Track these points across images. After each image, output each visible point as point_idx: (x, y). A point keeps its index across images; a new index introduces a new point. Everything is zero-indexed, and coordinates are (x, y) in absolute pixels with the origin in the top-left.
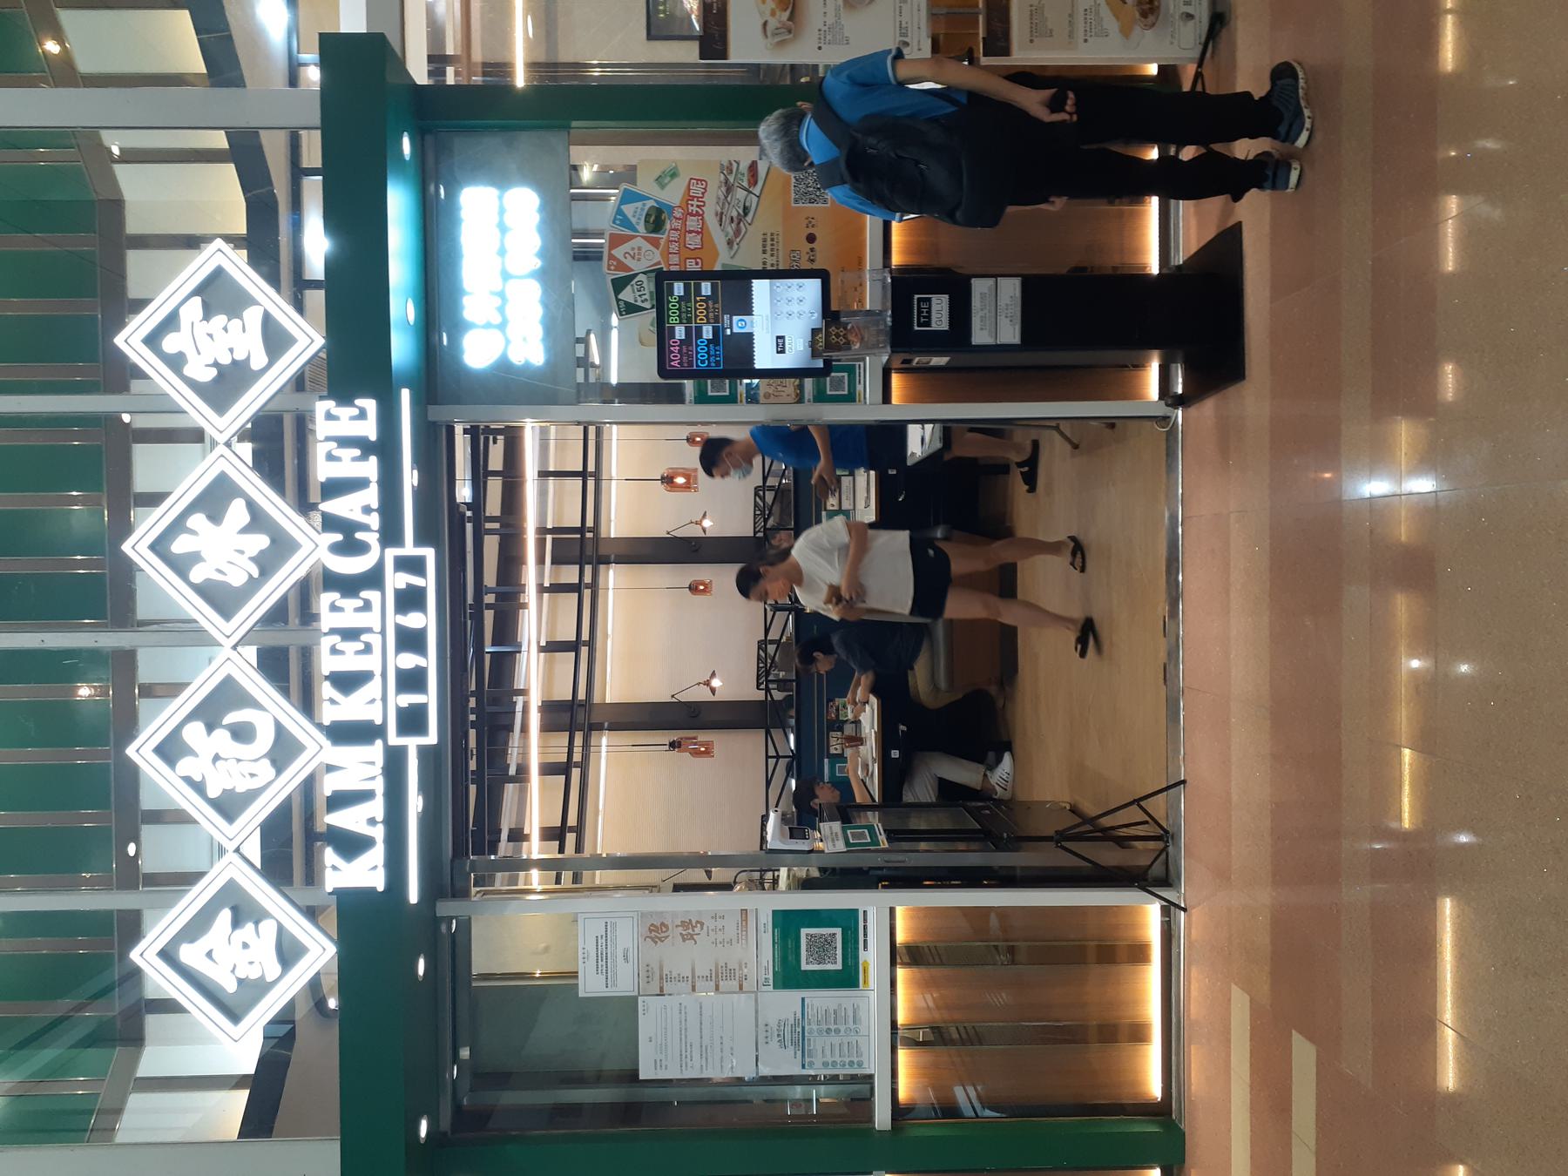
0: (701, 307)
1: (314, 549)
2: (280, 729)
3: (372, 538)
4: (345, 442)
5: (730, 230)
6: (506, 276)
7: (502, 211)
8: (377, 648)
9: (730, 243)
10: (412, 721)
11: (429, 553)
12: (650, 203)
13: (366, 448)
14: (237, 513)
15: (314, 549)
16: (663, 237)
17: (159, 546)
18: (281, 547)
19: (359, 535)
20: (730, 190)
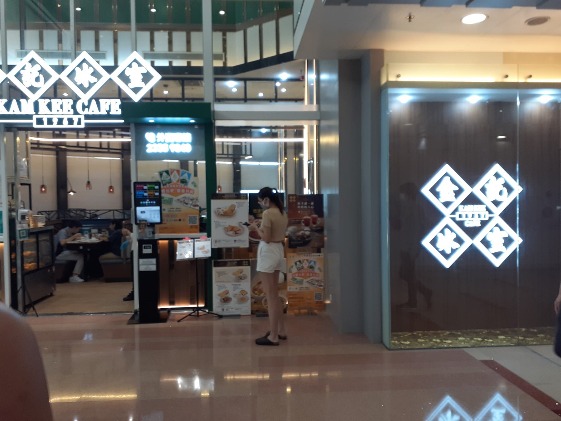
0: (152, 193)
1: (84, 98)
2: (38, 89)
3: (86, 112)
4: (110, 106)
5: (182, 200)
6: (169, 144)
7: (185, 143)
8: (58, 113)
9: (178, 200)
10: (40, 121)
11: (82, 126)
12: (188, 180)
13: (108, 112)
14: (93, 79)
15: (84, 98)
16: (179, 183)
17: (84, 61)
18: (85, 90)
19: (86, 109)
20: (192, 200)
